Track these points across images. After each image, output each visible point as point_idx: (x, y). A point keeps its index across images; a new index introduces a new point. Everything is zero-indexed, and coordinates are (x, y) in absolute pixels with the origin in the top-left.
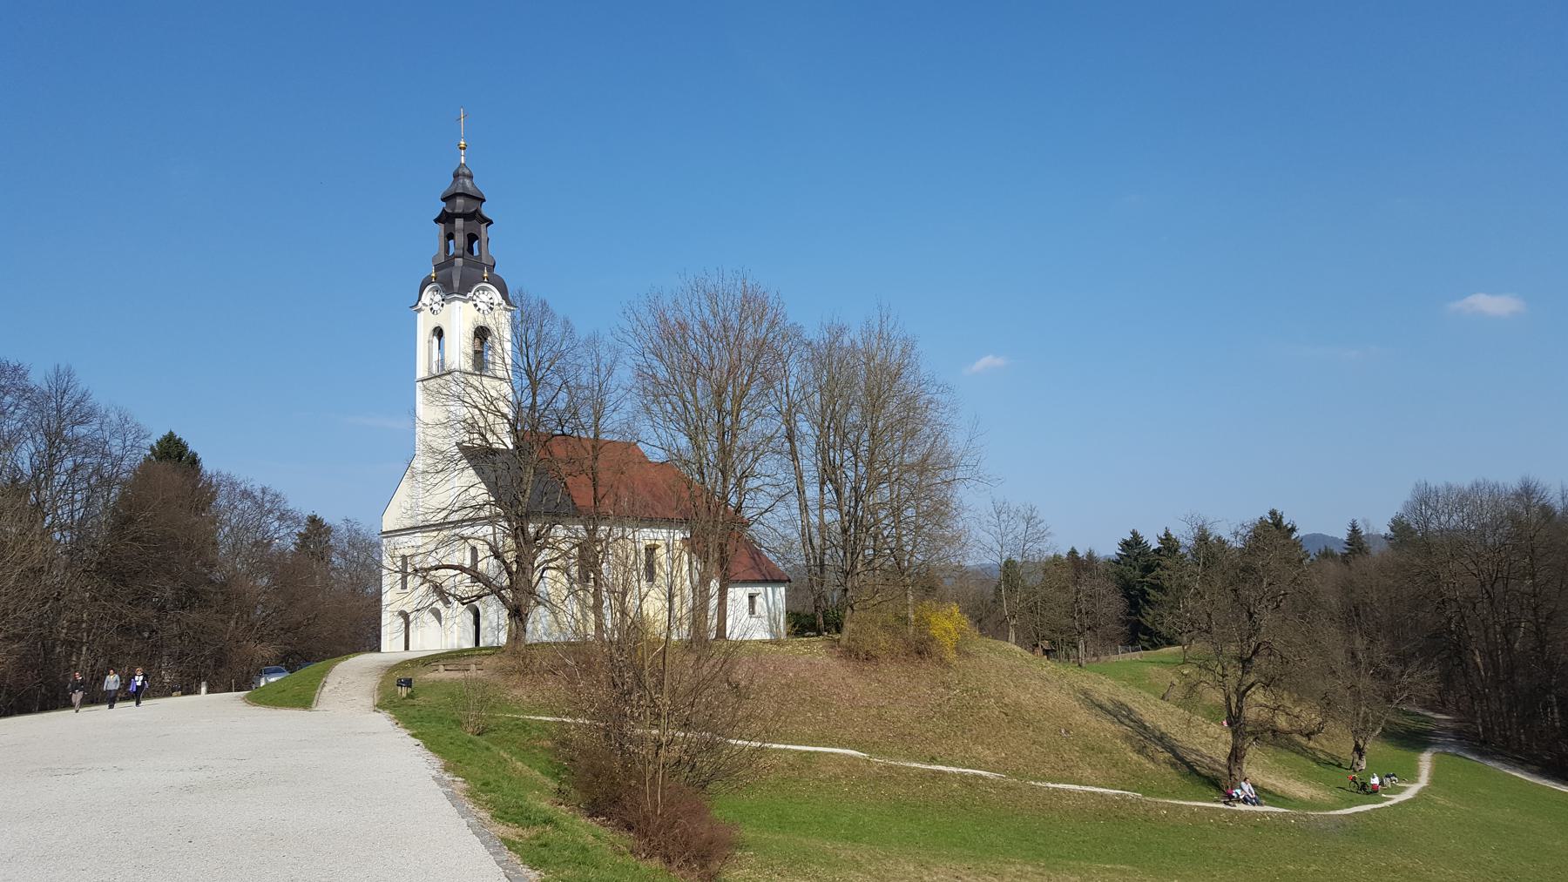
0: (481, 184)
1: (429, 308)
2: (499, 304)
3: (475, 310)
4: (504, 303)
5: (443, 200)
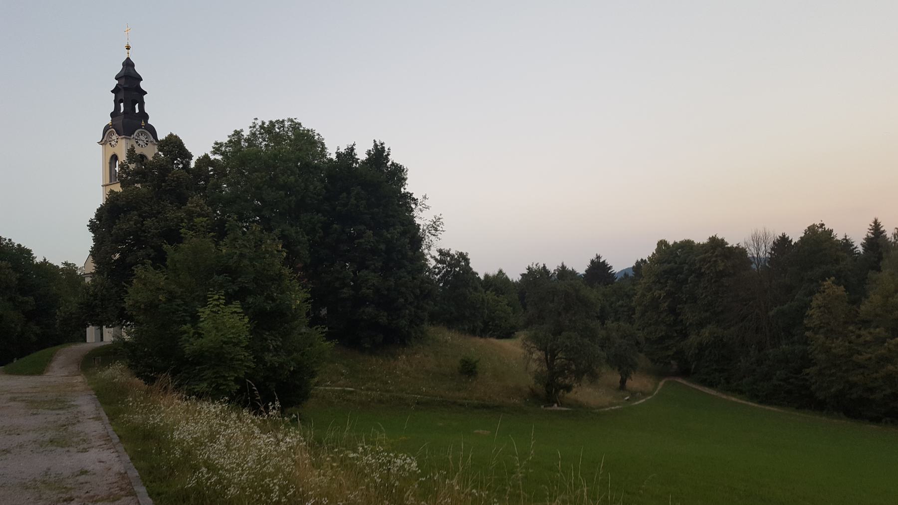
0: (138, 69)
1: (108, 143)
2: (151, 142)
4: (154, 141)
5: (116, 79)
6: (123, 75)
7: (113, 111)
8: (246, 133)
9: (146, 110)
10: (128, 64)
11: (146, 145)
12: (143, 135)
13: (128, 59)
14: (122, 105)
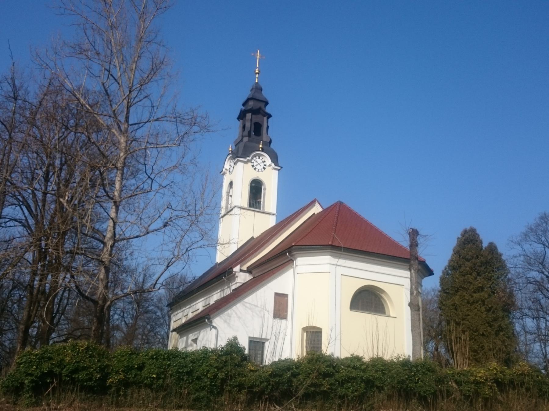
0: (266, 94)
3: (252, 169)
4: (273, 164)
11: (263, 170)
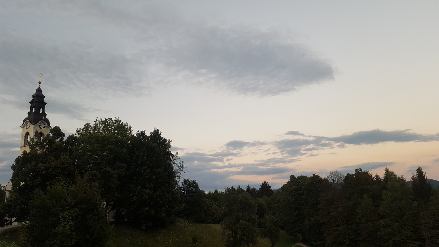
1: (25, 127)
2: (46, 126)
5: (32, 97)
6: (36, 95)
7: (29, 111)
8: (92, 124)
9: (46, 112)
10: (39, 90)
11: (44, 128)
12: (43, 123)
13: (39, 88)
14: (34, 109)
